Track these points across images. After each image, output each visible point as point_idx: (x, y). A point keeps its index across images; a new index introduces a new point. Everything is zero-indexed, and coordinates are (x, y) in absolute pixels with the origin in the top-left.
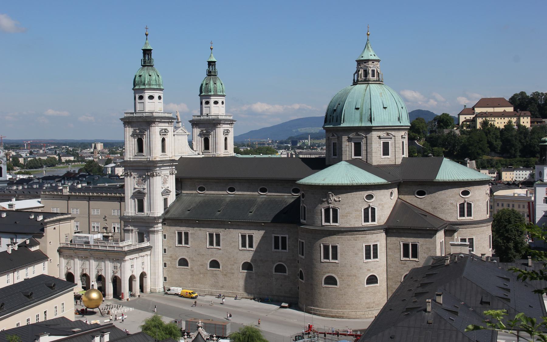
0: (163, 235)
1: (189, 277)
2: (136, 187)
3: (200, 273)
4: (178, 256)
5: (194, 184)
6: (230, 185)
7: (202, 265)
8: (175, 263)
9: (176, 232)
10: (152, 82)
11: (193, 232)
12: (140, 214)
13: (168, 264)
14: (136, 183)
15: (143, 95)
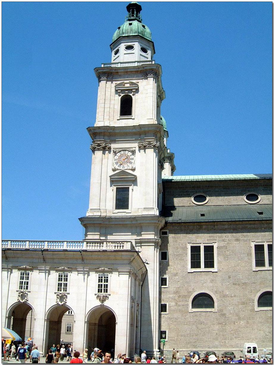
0: (161, 253)
1: (217, 327)
2: (117, 167)
3: (239, 319)
4: (191, 290)
5: (186, 192)
6: (248, 191)
7: (243, 303)
8: (186, 303)
9: (189, 247)
10: (146, 33)
11: (222, 244)
12: (122, 213)
13: (170, 307)
14: (115, 161)
15: (134, 45)
